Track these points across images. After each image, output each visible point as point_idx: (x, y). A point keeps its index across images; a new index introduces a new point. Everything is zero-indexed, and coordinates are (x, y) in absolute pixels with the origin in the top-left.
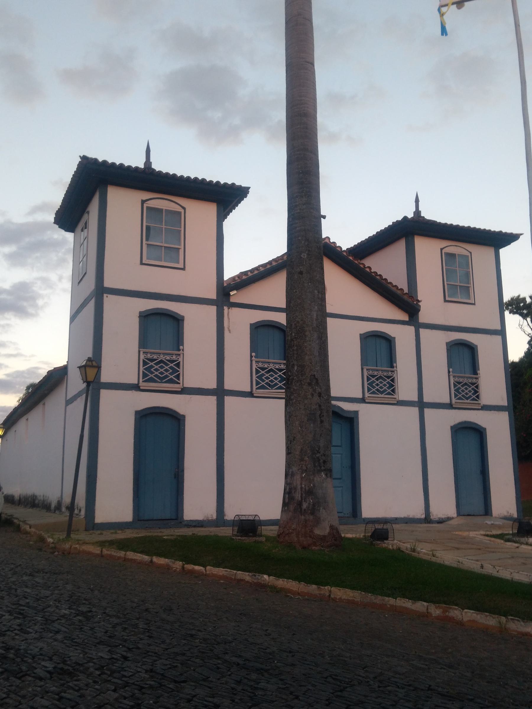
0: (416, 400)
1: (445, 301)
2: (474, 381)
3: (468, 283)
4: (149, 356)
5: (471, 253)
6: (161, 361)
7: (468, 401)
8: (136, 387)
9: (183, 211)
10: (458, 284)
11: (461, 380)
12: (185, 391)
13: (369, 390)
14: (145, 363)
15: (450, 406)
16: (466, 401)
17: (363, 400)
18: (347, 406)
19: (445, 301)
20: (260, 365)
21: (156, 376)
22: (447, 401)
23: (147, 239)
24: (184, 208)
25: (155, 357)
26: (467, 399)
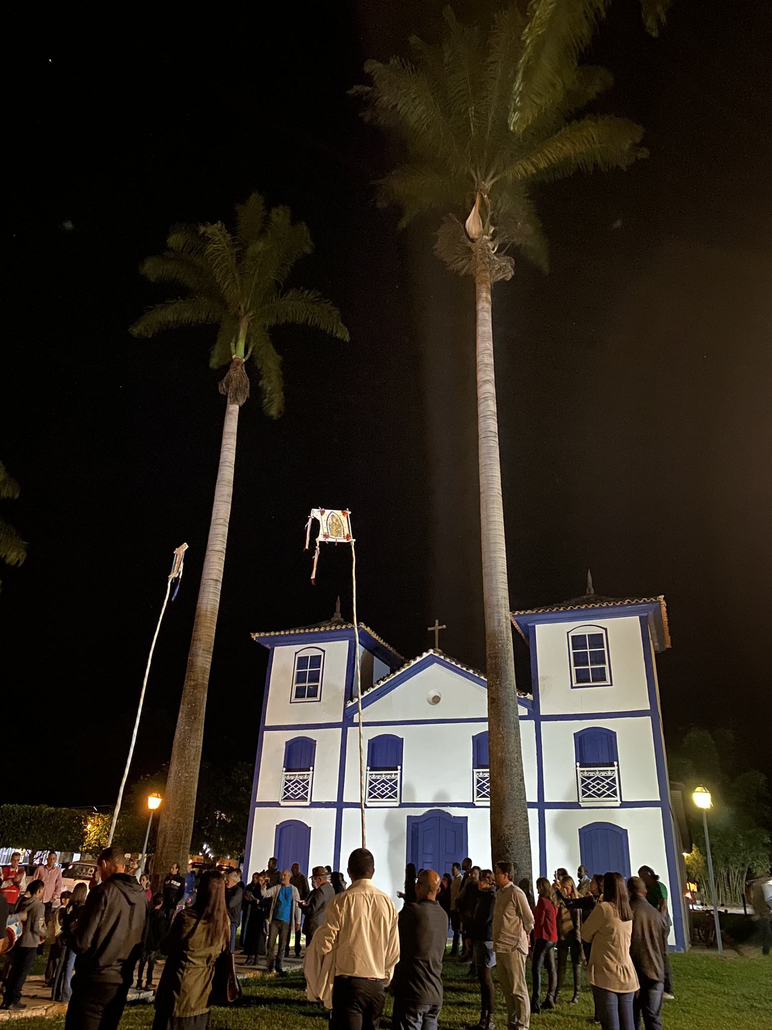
0: (536, 800)
1: (572, 687)
2: (609, 774)
3: (604, 663)
4: (288, 778)
5: (606, 629)
6: (297, 781)
7: (601, 798)
8: (277, 804)
9: (322, 654)
10: (590, 667)
11: (592, 774)
12: (314, 805)
13: (478, 793)
14: (286, 784)
15: (576, 806)
16: (598, 799)
17: (471, 805)
18: (456, 812)
19: (572, 687)
20: (374, 777)
21: (292, 794)
22: (575, 800)
23: (297, 682)
24: (324, 651)
25: (292, 778)
26: (599, 796)
